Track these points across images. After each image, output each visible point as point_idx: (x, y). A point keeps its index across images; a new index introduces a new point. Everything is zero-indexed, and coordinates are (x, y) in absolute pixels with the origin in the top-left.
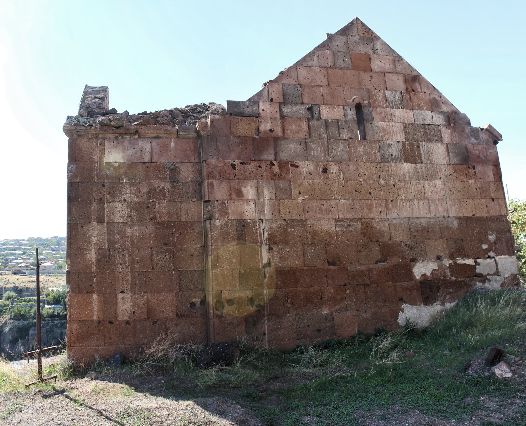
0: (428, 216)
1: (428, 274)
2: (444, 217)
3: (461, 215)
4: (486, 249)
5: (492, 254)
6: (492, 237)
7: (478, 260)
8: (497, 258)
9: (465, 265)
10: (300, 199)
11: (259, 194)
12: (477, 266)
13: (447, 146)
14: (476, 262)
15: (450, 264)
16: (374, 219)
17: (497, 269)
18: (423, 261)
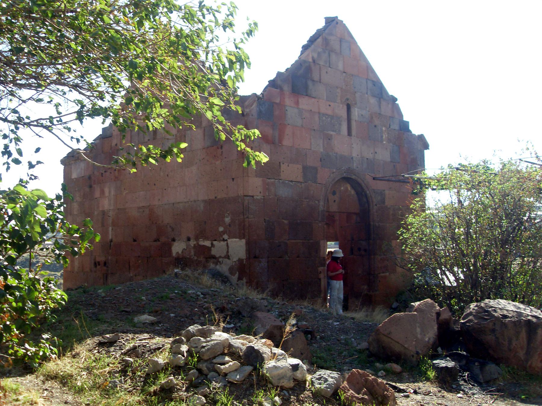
0: (185, 200)
1: (180, 252)
2: (195, 201)
3: (206, 198)
4: (222, 232)
5: (226, 237)
6: (227, 220)
7: (215, 243)
8: (229, 241)
9: (204, 246)
10: (124, 193)
11: (110, 192)
12: (212, 248)
13: (204, 130)
14: (212, 244)
15: (194, 245)
16: (155, 205)
17: (228, 252)
18: (179, 240)
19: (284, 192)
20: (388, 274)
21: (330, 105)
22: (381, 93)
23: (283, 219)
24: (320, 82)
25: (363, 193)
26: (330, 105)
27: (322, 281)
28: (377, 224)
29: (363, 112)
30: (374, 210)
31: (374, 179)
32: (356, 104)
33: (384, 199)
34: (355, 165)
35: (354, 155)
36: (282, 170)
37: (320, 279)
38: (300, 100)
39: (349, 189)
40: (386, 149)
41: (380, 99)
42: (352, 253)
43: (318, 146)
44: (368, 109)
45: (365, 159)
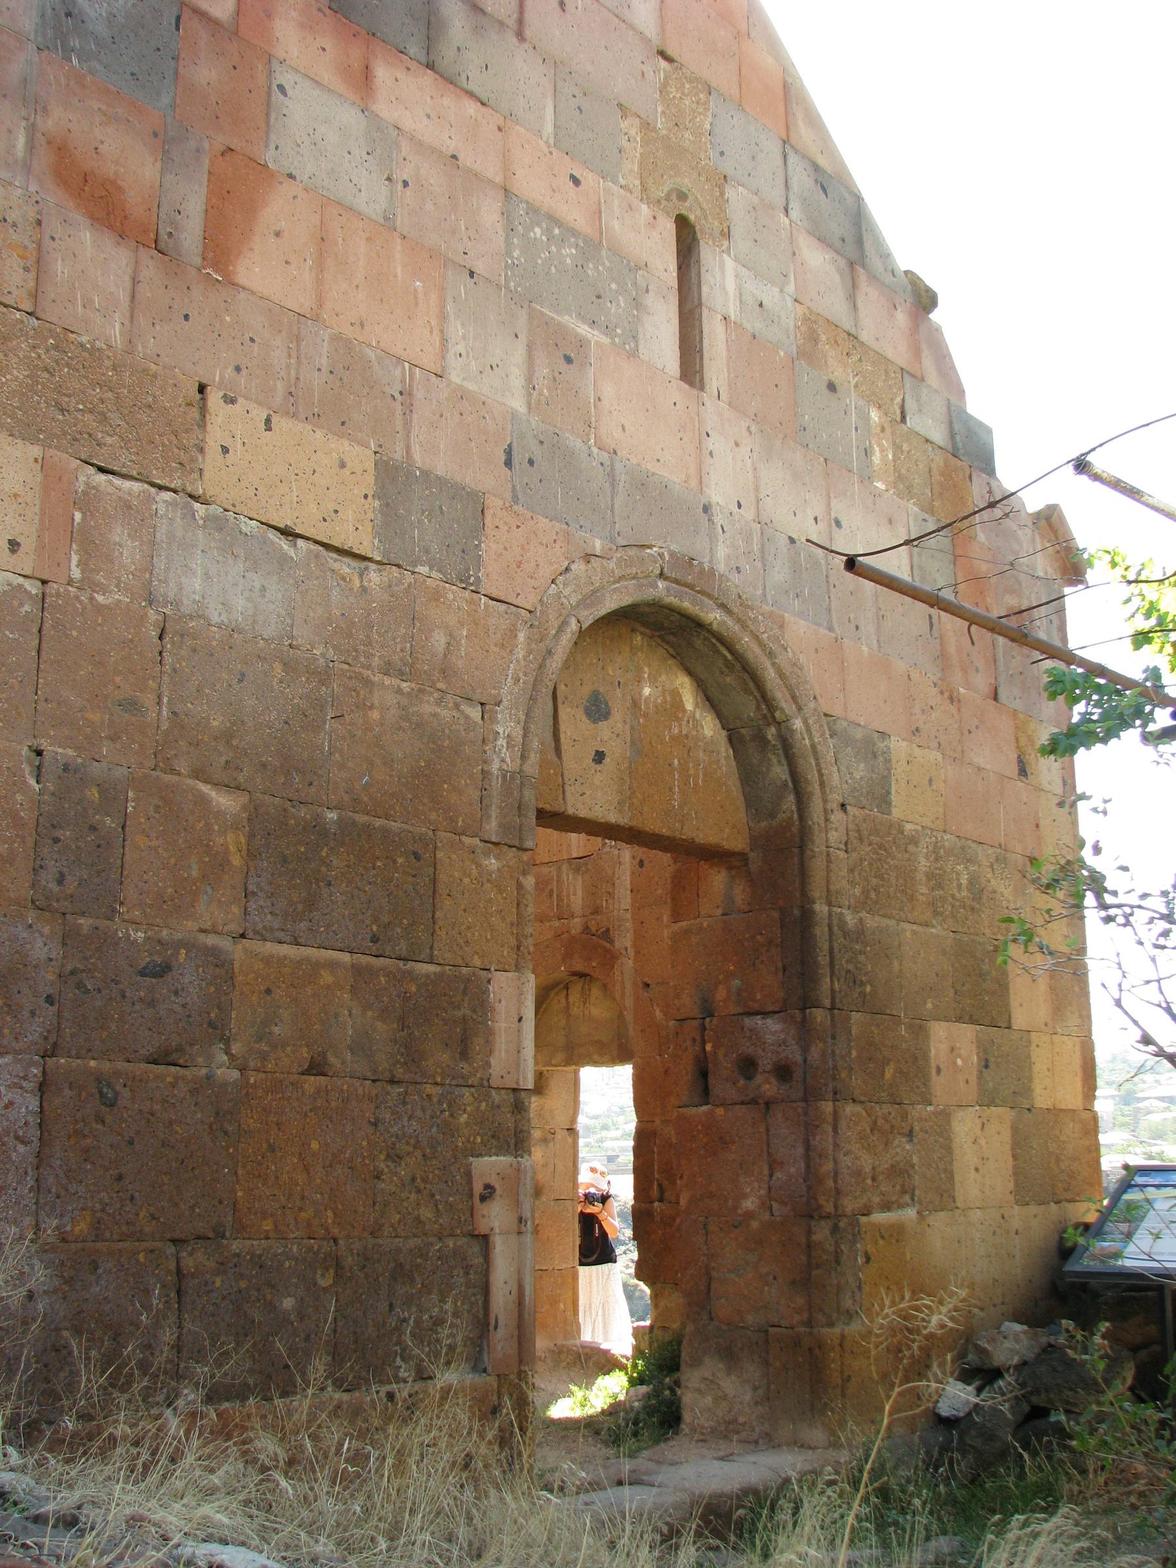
19: (220, 589)
20: (911, 1213)
21: (576, 181)
22: (860, 242)
23: (199, 774)
24: (520, 35)
25: (771, 733)
26: (576, 181)
27: (500, 1246)
28: (850, 919)
29: (770, 295)
30: (834, 836)
31: (851, 563)
32: (727, 234)
33: (885, 780)
34: (722, 552)
35: (719, 494)
36: (215, 436)
37: (485, 1240)
38: (383, 73)
39: (689, 699)
40: (890, 522)
41: (851, 264)
42: (705, 1094)
43: (494, 372)
44: (791, 288)
45: (783, 542)
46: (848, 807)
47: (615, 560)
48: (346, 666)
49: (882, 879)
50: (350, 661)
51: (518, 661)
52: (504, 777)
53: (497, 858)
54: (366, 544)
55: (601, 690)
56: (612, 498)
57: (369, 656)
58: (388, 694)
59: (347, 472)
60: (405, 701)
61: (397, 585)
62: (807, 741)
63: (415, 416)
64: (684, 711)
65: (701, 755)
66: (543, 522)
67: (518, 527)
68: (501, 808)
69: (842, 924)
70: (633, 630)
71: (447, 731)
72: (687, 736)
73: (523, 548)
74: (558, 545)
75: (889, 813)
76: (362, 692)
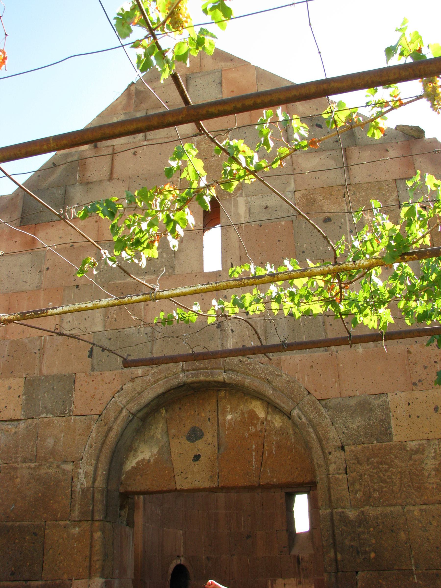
28: (352, 514)
46: (346, 447)
47: (150, 375)
48: (6, 465)
49: (384, 481)
50: (8, 462)
51: (92, 438)
52: (83, 491)
53: (79, 527)
54: (20, 414)
55: (197, 425)
56: (152, 346)
57: (16, 458)
58: (24, 471)
59: (12, 390)
60: (31, 471)
61: (30, 426)
62: (304, 419)
63: (45, 356)
64: (258, 418)
65: (275, 438)
66: (107, 374)
67: (93, 381)
68: (80, 505)
69: (344, 518)
70: (218, 390)
71: (52, 478)
72: (261, 431)
73: (96, 388)
74: (115, 381)
75: (391, 440)
76: (13, 473)
